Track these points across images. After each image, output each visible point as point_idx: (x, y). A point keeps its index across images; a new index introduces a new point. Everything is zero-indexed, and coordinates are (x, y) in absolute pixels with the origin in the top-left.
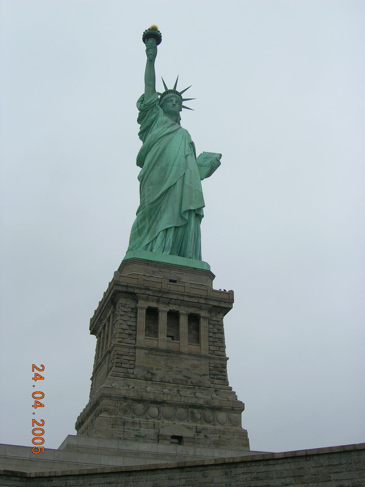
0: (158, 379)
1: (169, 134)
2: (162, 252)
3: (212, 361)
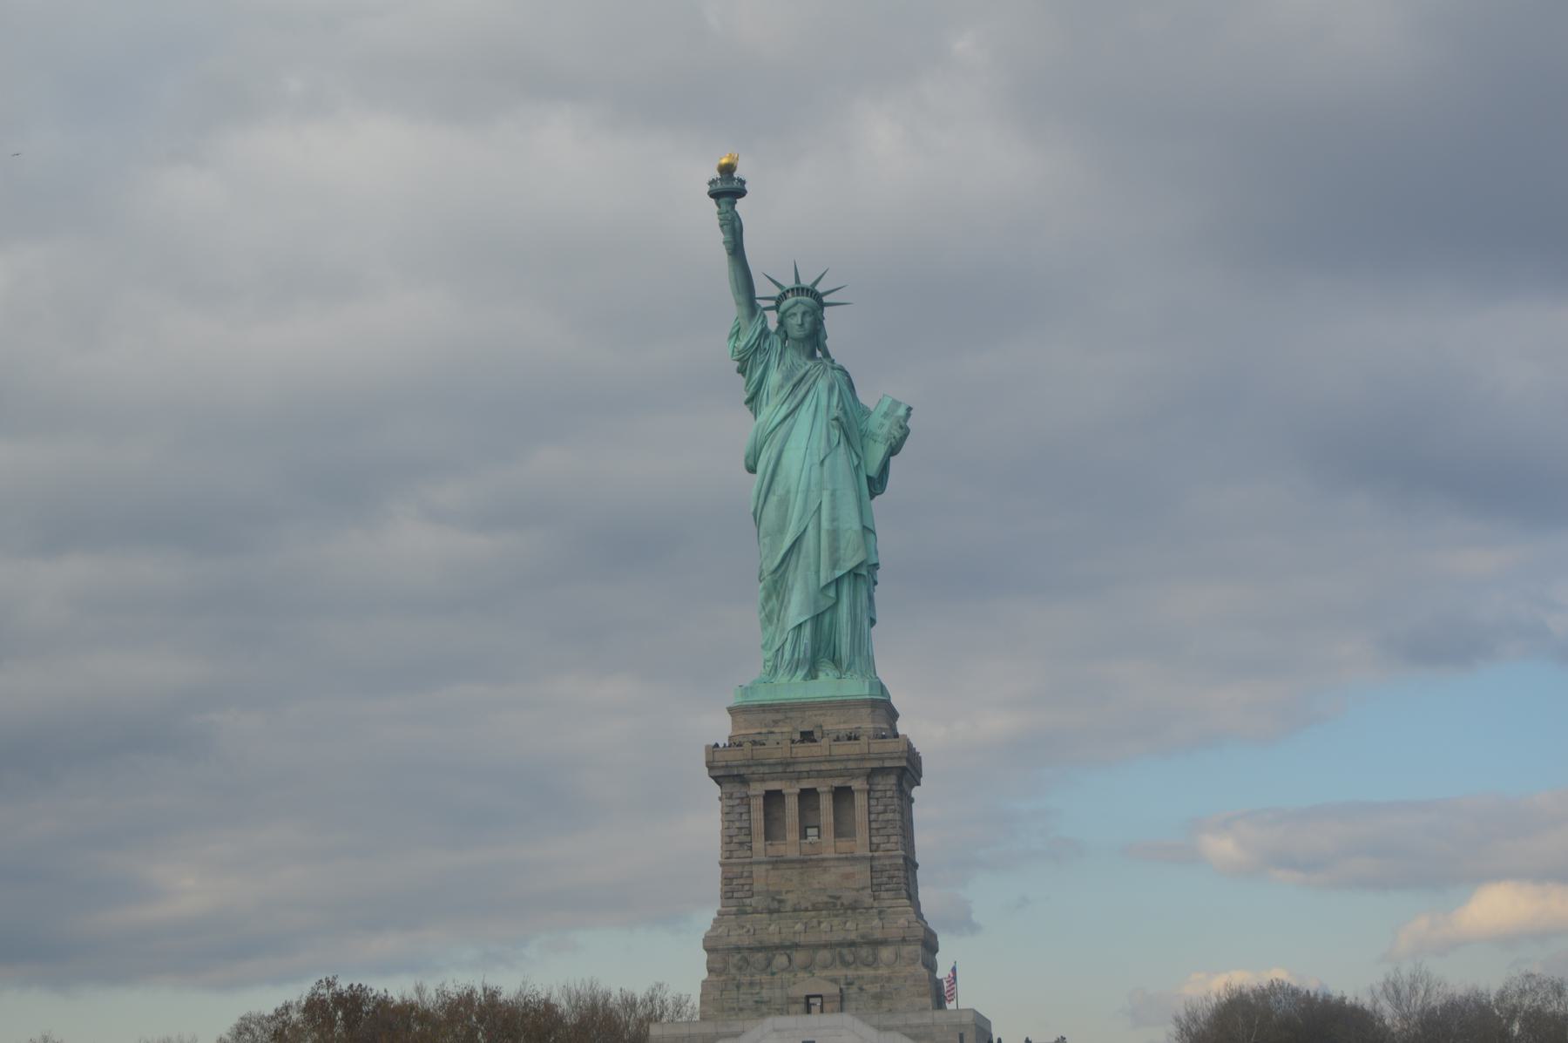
0: (788, 906)
1: (785, 418)
2: (792, 672)
3: (876, 863)
